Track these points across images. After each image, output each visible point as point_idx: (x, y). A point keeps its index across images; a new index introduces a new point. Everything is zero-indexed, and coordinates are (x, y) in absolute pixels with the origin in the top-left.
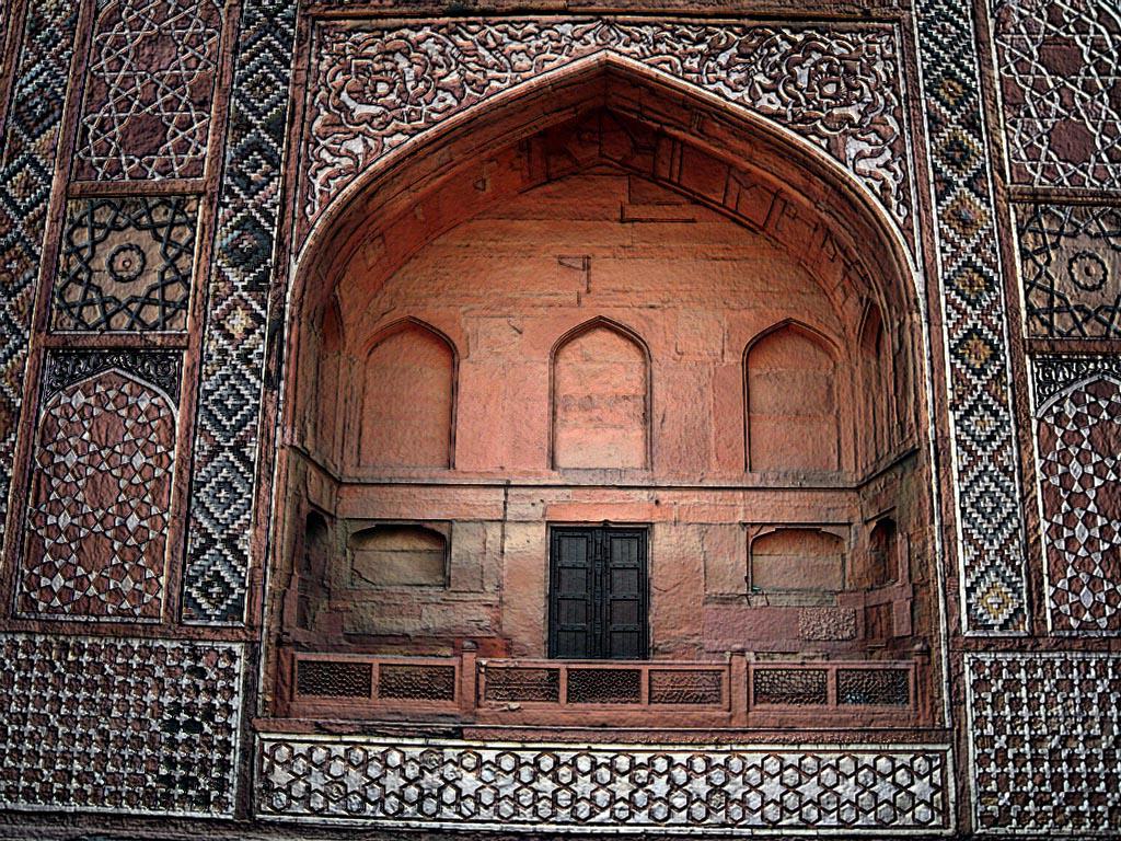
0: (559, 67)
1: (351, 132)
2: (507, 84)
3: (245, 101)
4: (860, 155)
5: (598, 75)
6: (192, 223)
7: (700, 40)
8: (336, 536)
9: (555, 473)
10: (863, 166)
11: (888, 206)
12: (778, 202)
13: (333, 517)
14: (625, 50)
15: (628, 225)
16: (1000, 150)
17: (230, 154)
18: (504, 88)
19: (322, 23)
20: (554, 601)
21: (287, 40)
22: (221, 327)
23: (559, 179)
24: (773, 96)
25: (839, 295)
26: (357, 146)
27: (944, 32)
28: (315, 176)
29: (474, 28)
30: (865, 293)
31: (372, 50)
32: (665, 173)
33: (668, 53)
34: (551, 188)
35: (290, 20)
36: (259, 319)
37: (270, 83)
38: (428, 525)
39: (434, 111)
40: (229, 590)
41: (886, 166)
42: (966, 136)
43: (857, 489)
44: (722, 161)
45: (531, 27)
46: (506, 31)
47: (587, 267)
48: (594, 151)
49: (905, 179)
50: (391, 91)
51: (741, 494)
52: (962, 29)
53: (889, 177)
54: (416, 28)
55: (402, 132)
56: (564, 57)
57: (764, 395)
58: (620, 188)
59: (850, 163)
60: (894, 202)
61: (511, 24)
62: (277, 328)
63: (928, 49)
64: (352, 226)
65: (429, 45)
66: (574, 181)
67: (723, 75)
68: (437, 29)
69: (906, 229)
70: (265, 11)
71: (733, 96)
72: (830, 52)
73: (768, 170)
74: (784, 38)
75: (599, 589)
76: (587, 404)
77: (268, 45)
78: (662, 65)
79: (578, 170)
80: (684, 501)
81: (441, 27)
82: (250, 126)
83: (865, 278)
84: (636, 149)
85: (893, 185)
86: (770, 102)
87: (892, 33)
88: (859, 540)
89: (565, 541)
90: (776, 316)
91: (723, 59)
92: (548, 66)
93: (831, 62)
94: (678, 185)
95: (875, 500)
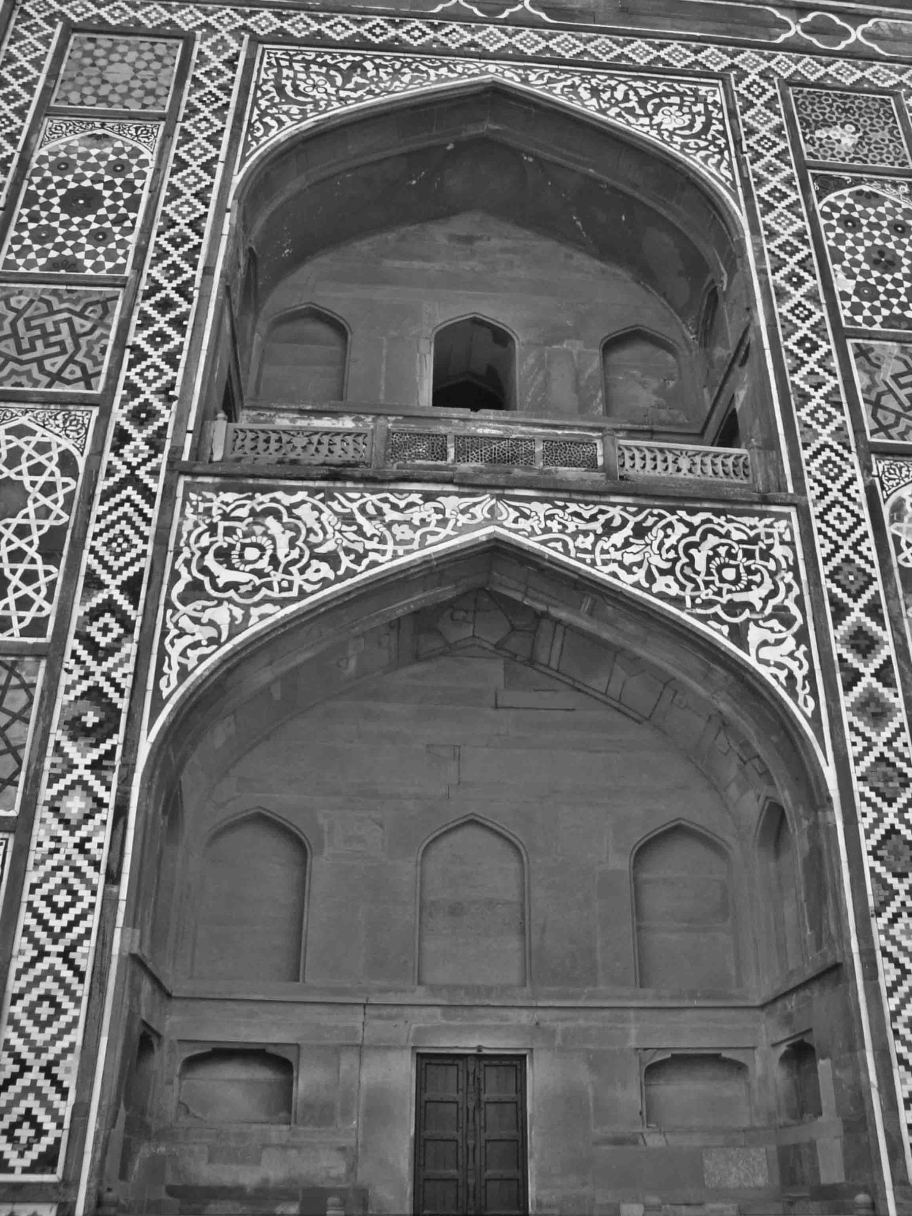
0: (443, 542)
1: (213, 599)
2: (389, 555)
3: (101, 559)
4: (765, 643)
5: (485, 551)
6: (28, 688)
7: (593, 518)
8: (164, 1062)
9: (421, 990)
10: (771, 654)
11: (794, 695)
12: (668, 694)
13: (159, 1036)
14: (514, 526)
15: (502, 711)
16: (905, 640)
17: (78, 611)
18: (388, 560)
19: (188, 479)
20: (421, 1145)
21: (149, 497)
22: (55, 810)
23: (428, 659)
24: (670, 579)
25: (733, 791)
26: (221, 615)
27: (839, 518)
28: (172, 644)
29: (352, 495)
30: (765, 790)
31: (243, 512)
32: (543, 658)
33: (560, 532)
34: (418, 668)
35: (154, 473)
36: (100, 804)
37: (127, 539)
38: (271, 1050)
39: (307, 581)
40: (41, 1132)
41: (791, 655)
42: (870, 624)
43: (762, 1007)
44: (606, 645)
45: (415, 498)
46: (385, 500)
47: (457, 757)
48: (468, 631)
49: (812, 670)
50: (261, 557)
51: (632, 1014)
52: (857, 516)
53: (794, 665)
54: (291, 491)
55: (274, 601)
56: (448, 531)
57: (658, 901)
58: (495, 670)
59: (752, 650)
60: (801, 694)
61: (392, 492)
62: (121, 811)
63: (825, 535)
64: (203, 704)
65: (304, 511)
66: (443, 660)
67: (617, 555)
68: (313, 492)
69: (815, 720)
70: (128, 464)
71: (631, 579)
72: (728, 535)
73: (659, 655)
74: (681, 520)
75: (471, 1127)
76: (456, 910)
77: (128, 499)
78: (552, 544)
79: (449, 650)
80: (569, 1024)
81: (318, 491)
82: (102, 586)
83: (765, 773)
84: (513, 629)
85: (799, 675)
86: (668, 586)
87: (787, 517)
88: (767, 1068)
89: (432, 1069)
90: (667, 811)
91: (618, 539)
92: (431, 539)
93: (731, 547)
94: (558, 671)
95: (788, 1019)
